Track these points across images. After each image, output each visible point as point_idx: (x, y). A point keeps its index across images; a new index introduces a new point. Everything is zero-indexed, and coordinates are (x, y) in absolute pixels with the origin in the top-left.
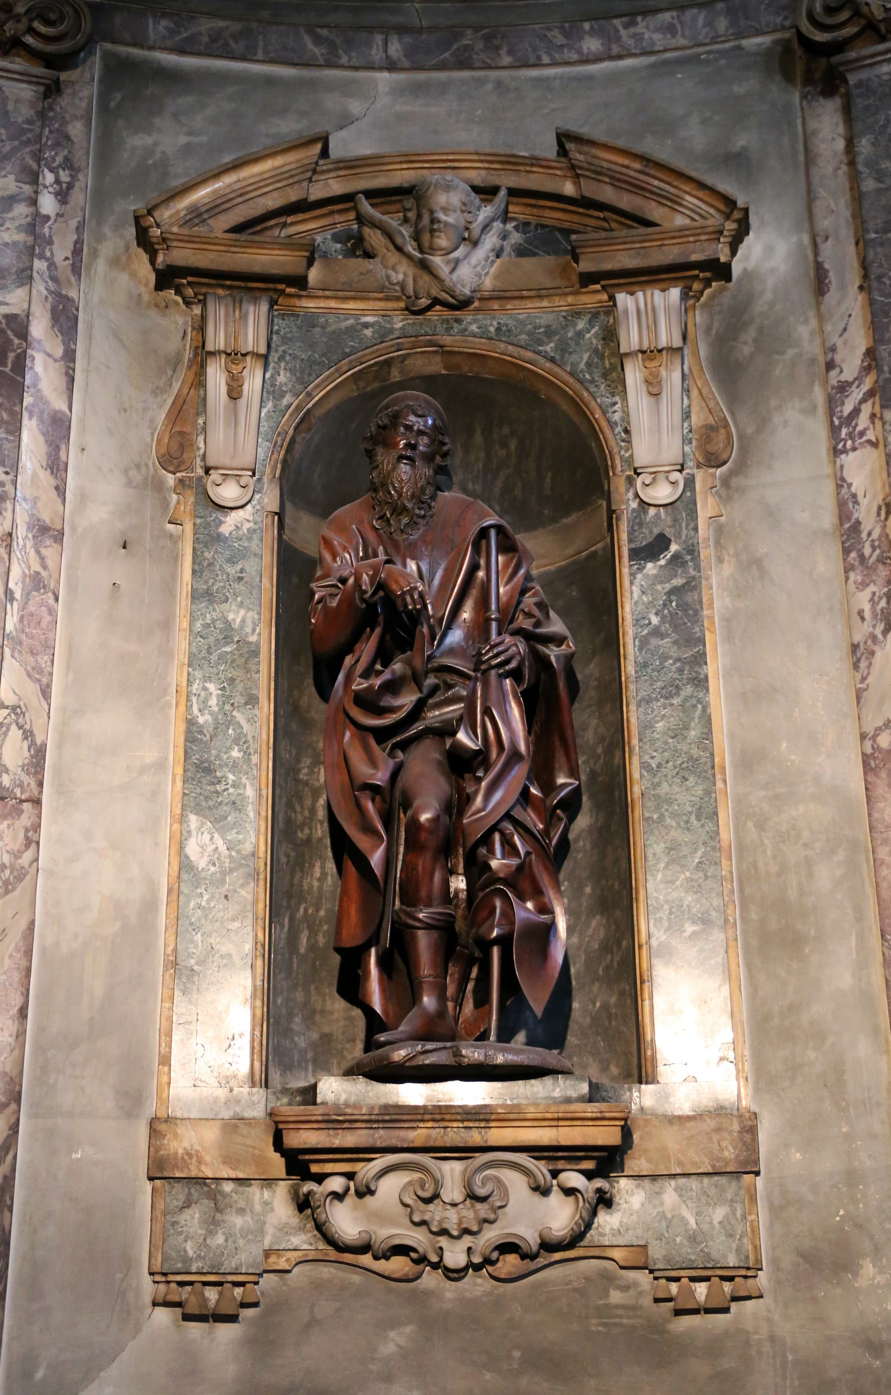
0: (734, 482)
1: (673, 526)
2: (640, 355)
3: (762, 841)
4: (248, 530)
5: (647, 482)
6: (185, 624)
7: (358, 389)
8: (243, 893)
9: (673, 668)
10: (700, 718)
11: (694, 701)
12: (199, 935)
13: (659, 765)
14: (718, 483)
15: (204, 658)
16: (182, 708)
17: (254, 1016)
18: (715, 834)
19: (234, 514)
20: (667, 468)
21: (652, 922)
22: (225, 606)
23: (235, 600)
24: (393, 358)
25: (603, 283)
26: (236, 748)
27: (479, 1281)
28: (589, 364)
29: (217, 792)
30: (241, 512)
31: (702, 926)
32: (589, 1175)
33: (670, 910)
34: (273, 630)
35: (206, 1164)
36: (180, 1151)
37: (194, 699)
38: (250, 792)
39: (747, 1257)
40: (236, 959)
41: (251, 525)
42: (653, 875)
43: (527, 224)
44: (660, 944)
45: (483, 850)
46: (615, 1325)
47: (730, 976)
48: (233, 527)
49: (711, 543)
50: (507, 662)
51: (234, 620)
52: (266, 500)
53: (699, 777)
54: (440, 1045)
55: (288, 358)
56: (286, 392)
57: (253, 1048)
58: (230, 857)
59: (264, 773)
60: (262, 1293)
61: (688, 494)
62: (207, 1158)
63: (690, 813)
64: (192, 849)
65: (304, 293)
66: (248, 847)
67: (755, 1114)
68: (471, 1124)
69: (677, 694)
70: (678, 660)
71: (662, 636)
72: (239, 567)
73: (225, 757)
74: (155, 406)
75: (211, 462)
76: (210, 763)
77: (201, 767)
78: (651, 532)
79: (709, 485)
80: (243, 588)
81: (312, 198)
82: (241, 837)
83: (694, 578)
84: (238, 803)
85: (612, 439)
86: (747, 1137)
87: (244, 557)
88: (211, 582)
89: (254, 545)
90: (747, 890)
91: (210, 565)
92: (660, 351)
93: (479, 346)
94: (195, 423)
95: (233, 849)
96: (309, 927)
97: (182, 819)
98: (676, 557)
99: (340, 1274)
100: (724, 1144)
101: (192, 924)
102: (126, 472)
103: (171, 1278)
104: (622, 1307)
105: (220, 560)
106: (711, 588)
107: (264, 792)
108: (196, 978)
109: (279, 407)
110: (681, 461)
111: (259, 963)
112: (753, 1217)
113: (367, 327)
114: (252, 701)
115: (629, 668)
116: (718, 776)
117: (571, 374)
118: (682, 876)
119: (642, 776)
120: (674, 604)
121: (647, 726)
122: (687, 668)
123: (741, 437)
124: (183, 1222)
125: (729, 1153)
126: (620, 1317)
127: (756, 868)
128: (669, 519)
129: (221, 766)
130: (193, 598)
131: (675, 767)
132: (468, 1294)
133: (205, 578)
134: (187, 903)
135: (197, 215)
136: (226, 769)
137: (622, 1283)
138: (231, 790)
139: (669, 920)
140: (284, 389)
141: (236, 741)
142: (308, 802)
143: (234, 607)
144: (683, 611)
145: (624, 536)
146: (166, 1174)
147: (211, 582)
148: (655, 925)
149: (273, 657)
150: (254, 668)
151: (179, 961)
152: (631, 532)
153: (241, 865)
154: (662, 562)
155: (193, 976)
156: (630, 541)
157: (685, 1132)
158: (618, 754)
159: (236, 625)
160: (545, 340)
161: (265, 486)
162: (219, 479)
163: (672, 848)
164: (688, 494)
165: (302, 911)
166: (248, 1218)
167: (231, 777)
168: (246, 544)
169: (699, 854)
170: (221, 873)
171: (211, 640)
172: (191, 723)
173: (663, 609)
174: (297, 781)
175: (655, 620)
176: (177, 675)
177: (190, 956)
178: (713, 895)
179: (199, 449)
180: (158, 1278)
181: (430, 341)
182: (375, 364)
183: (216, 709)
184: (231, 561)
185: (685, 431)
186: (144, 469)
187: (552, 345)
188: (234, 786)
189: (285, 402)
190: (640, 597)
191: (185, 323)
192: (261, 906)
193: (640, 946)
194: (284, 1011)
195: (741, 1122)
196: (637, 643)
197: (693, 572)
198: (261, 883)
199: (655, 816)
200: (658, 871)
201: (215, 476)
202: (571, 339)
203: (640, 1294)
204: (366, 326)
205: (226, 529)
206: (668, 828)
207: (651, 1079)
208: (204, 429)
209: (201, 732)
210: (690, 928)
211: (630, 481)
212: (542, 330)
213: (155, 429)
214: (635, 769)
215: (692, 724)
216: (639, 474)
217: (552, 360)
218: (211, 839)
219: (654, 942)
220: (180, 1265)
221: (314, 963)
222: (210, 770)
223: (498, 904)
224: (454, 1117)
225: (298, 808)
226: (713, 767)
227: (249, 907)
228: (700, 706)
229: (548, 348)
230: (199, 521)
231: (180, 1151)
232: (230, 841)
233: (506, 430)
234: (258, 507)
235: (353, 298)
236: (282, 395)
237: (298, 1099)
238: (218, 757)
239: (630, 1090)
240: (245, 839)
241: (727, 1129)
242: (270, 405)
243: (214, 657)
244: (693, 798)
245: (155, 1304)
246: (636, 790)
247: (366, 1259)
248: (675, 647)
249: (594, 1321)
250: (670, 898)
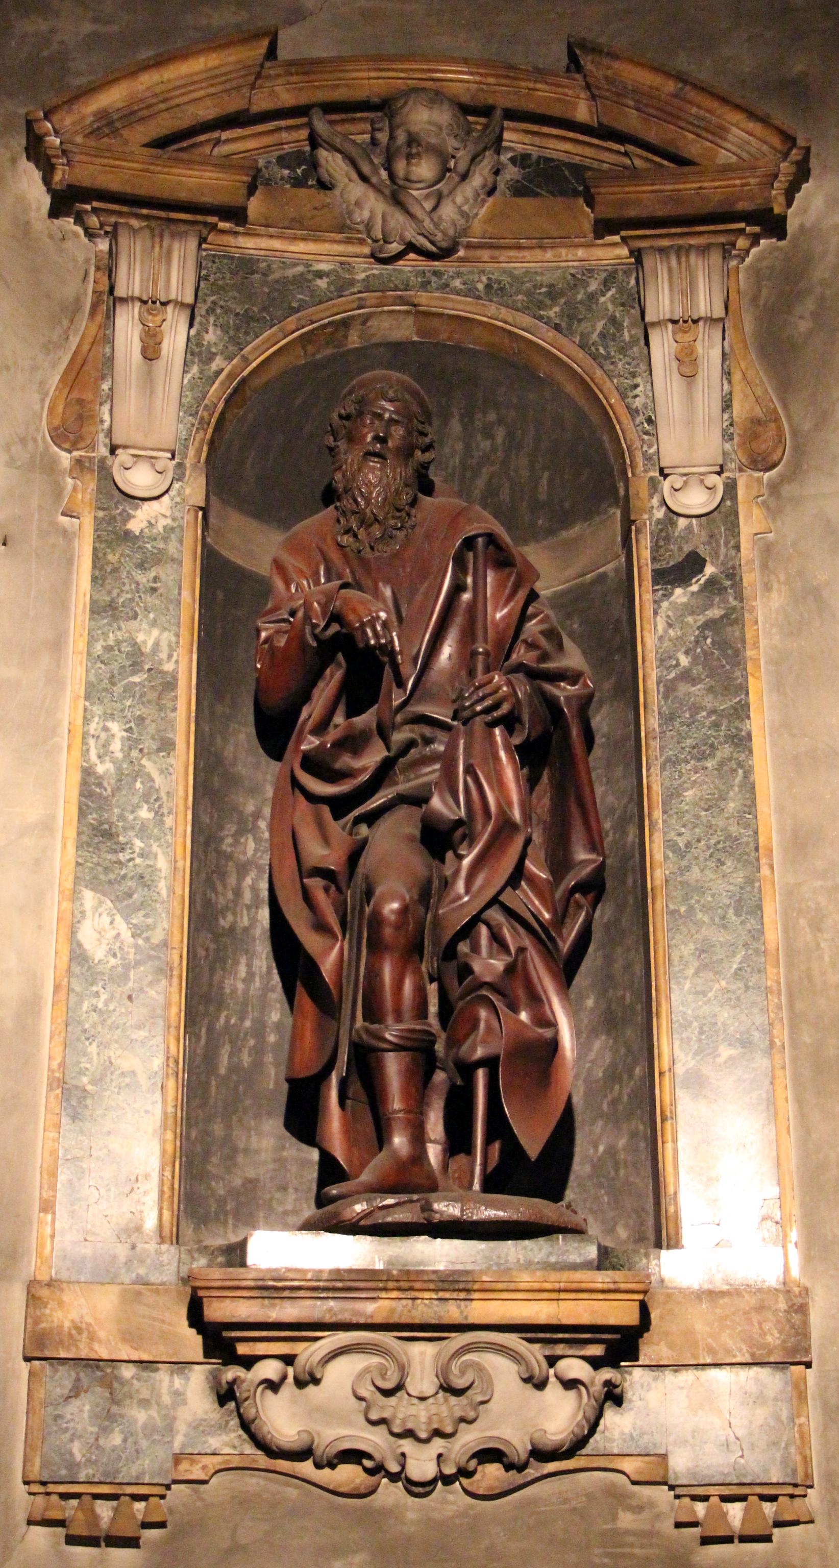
0: (787, 490)
1: (709, 543)
2: (670, 326)
3: (818, 945)
4: (165, 527)
5: (677, 486)
6: (82, 645)
7: (305, 354)
8: (152, 993)
9: (707, 723)
10: (740, 786)
11: (733, 764)
12: (94, 1045)
13: (688, 845)
14: (765, 490)
15: (106, 690)
16: (76, 753)
17: (164, 1152)
18: (758, 934)
19: (146, 506)
20: (702, 470)
21: (677, 1044)
22: (133, 624)
23: (146, 617)
24: (353, 317)
25: (623, 233)
26: (146, 807)
27: (451, 1497)
28: (603, 335)
29: (120, 863)
30: (154, 504)
31: (740, 1050)
32: (595, 1363)
33: (701, 1028)
34: (195, 657)
35: (100, 1342)
36: (67, 1324)
37: (92, 742)
38: (162, 863)
39: (794, 1471)
40: (143, 1079)
41: (169, 521)
42: (679, 983)
43: (526, 157)
44: (687, 1072)
45: (463, 947)
46: (624, 1555)
47: (776, 1114)
48: (145, 524)
49: (757, 564)
50: (496, 706)
51: (145, 642)
52: (188, 491)
53: (739, 861)
54: (404, 1198)
55: (219, 311)
56: (215, 354)
57: (162, 1193)
58: (136, 946)
59: (180, 840)
60: (171, 1511)
61: (728, 503)
62: (102, 1334)
63: (728, 906)
64: (87, 935)
65: (241, 229)
66: (157, 936)
67: (807, 1290)
68: (447, 1295)
69: (712, 755)
70: (713, 712)
71: (694, 681)
72: (152, 574)
73: (131, 817)
74: (46, 364)
75: (117, 440)
76: (111, 824)
77: (99, 832)
78: (680, 549)
79: (755, 493)
80: (157, 602)
81: (255, 109)
82: (150, 921)
83: (734, 609)
84: (147, 877)
85: (629, 430)
86: (796, 1318)
87: (158, 562)
88: (115, 593)
89: (172, 548)
90: (799, 1006)
91: (115, 570)
92: (695, 322)
93: (462, 306)
94: (97, 390)
95: (139, 935)
96: (231, 1042)
97: (75, 896)
98: (712, 582)
99: (273, 1487)
100: (766, 1326)
101: (85, 1031)
102: (8, 447)
103: (51, 1488)
104: (635, 1533)
105: (129, 565)
106: (756, 623)
107: (180, 864)
108: (89, 1102)
109: (207, 373)
110: (721, 462)
111: (171, 1083)
112: (802, 1420)
113: (321, 277)
114: (166, 746)
115: (650, 721)
116: (763, 861)
117: (581, 346)
118: (717, 986)
119: (666, 858)
120: (709, 641)
121: (672, 795)
122: (725, 722)
123: (795, 434)
124: (69, 1417)
125: (773, 1338)
126: (632, 1545)
127: (810, 977)
128: (703, 533)
129: (125, 829)
130: (92, 612)
131: (709, 848)
132: (436, 1515)
133: (108, 587)
134: (80, 1003)
135: (107, 125)
136: (131, 833)
137: (634, 1503)
138: (138, 861)
139: (700, 1040)
140: (214, 350)
141: (146, 798)
142: (232, 880)
143: (145, 626)
144: (722, 651)
145: (646, 554)
146: (47, 1354)
147: (115, 593)
148: (681, 1046)
149: (194, 691)
150: (170, 705)
151: (67, 1078)
152: (656, 548)
153: (150, 958)
154: (695, 588)
155: (85, 1098)
156: (654, 559)
157: (718, 1311)
158: (632, 831)
159: (147, 649)
160: (549, 302)
161: (188, 473)
162: (129, 461)
163: (704, 950)
164: (728, 503)
165: (222, 1020)
166: (154, 1413)
167: (138, 844)
168: (161, 545)
169: (738, 958)
170: (123, 966)
171: (115, 666)
172: (87, 772)
173: (695, 647)
174: (218, 852)
175: (684, 661)
176: (70, 707)
177: (82, 1072)
178: (755, 1010)
179: (102, 421)
180: (36, 1488)
181: (401, 297)
182: (329, 323)
183: (119, 755)
184: (141, 566)
185: (726, 424)
186: (31, 445)
187: (557, 309)
188: (141, 855)
189: (214, 366)
190: (666, 631)
191: (87, 261)
192: (174, 1010)
193: (661, 1074)
194: (199, 1148)
195: (788, 1299)
196: (661, 689)
197: (733, 602)
198: (175, 981)
199: (683, 909)
200: (686, 978)
201: (123, 456)
202: (580, 303)
203: (658, 1516)
204: (320, 275)
205: (135, 526)
206: (700, 924)
207: (675, 1243)
208: (111, 397)
209: (100, 785)
210: (725, 1052)
211: (654, 486)
212: (544, 290)
213: (46, 394)
214: (656, 848)
215: (731, 793)
216: (665, 476)
217: (557, 328)
218: (112, 923)
219: (679, 1069)
220: (64, 1472)
221: (236, 1088)
222: (111, 835)
223: (483, 1013)
224: (425, 1286)
225: (220, 888)
226: (757, 849)
227: (159, 1012)
228: (740, 771)
229: (551, 313)
230: (101, 514)
231: (67, 1324)
232: (135, 925)
233: (492, 416)
234: (178, 499)
235: (304, 239)
236: (211, 357)
237: (220, 1259)
238: (121, 817)
239: (647, 1255)
240: (155, 923)
241: (769, 1308)
242: (195, 369)
243: (118, 689)
244: (731, 888)
245: (30, 1523)
246: (659, 872)
247: (306, 1468)
248: (711, 697)
249: (597, 1551)
250: (700, 1013)
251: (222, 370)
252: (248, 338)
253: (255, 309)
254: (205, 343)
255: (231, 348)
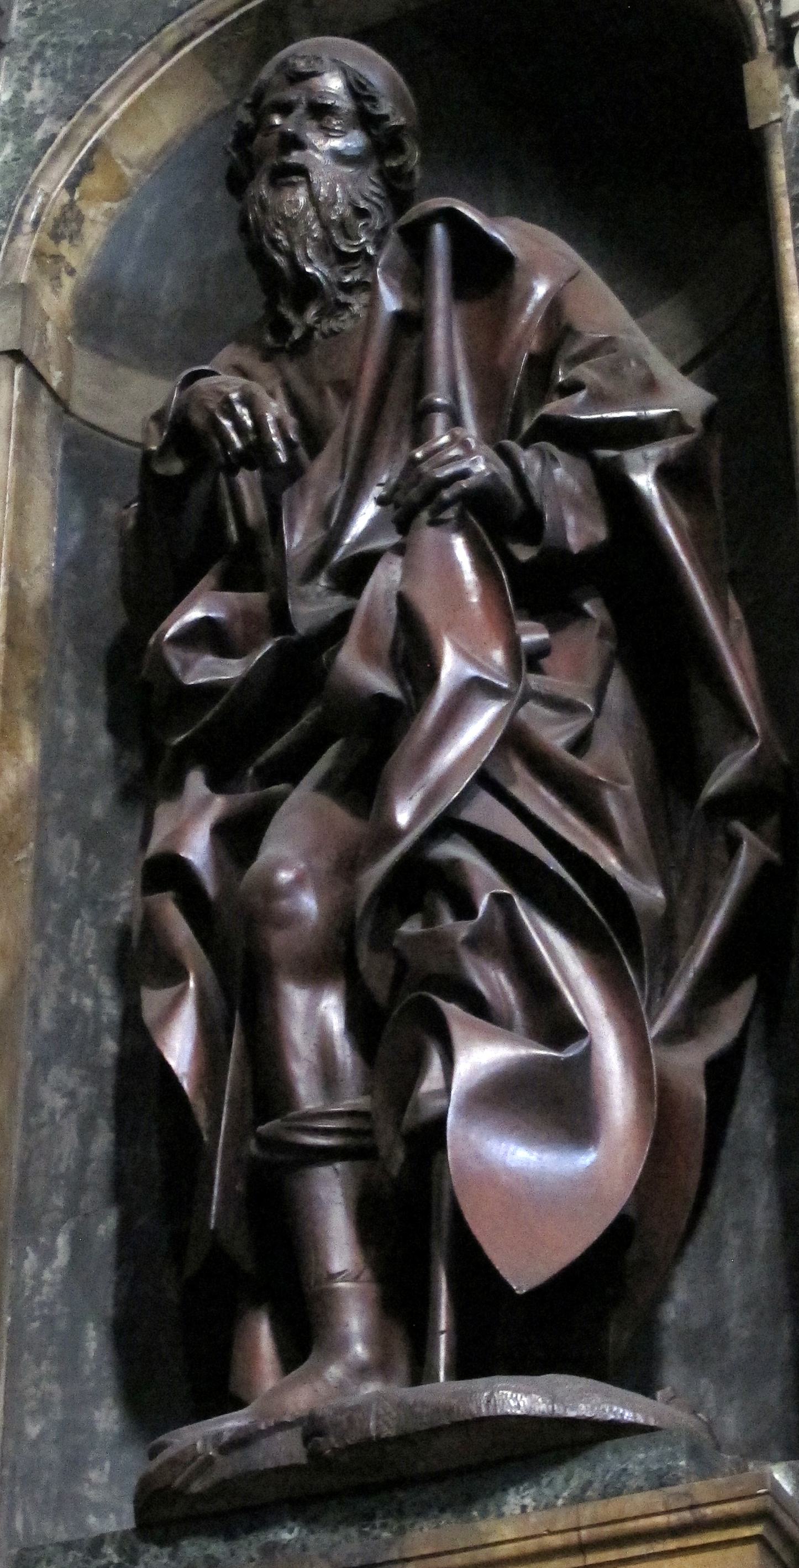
55: (49, 53)
56: (43, 116)
109: (26, 150)
189: (39, 135)
236: (35, 122)
251: (54, 136)
252: (97, 77)
253: (110, 32)
254: (26, 106)
255: (67, 100)
